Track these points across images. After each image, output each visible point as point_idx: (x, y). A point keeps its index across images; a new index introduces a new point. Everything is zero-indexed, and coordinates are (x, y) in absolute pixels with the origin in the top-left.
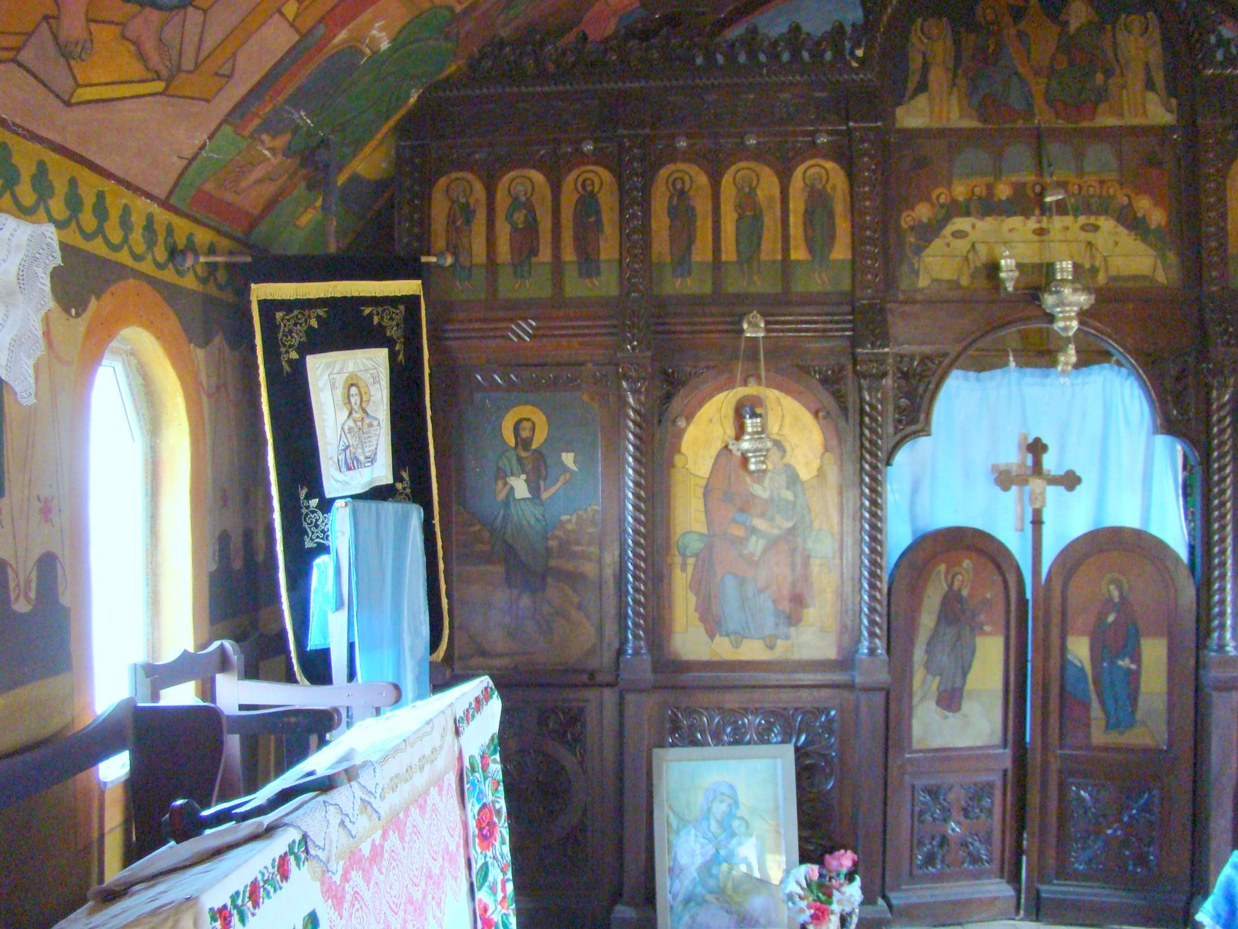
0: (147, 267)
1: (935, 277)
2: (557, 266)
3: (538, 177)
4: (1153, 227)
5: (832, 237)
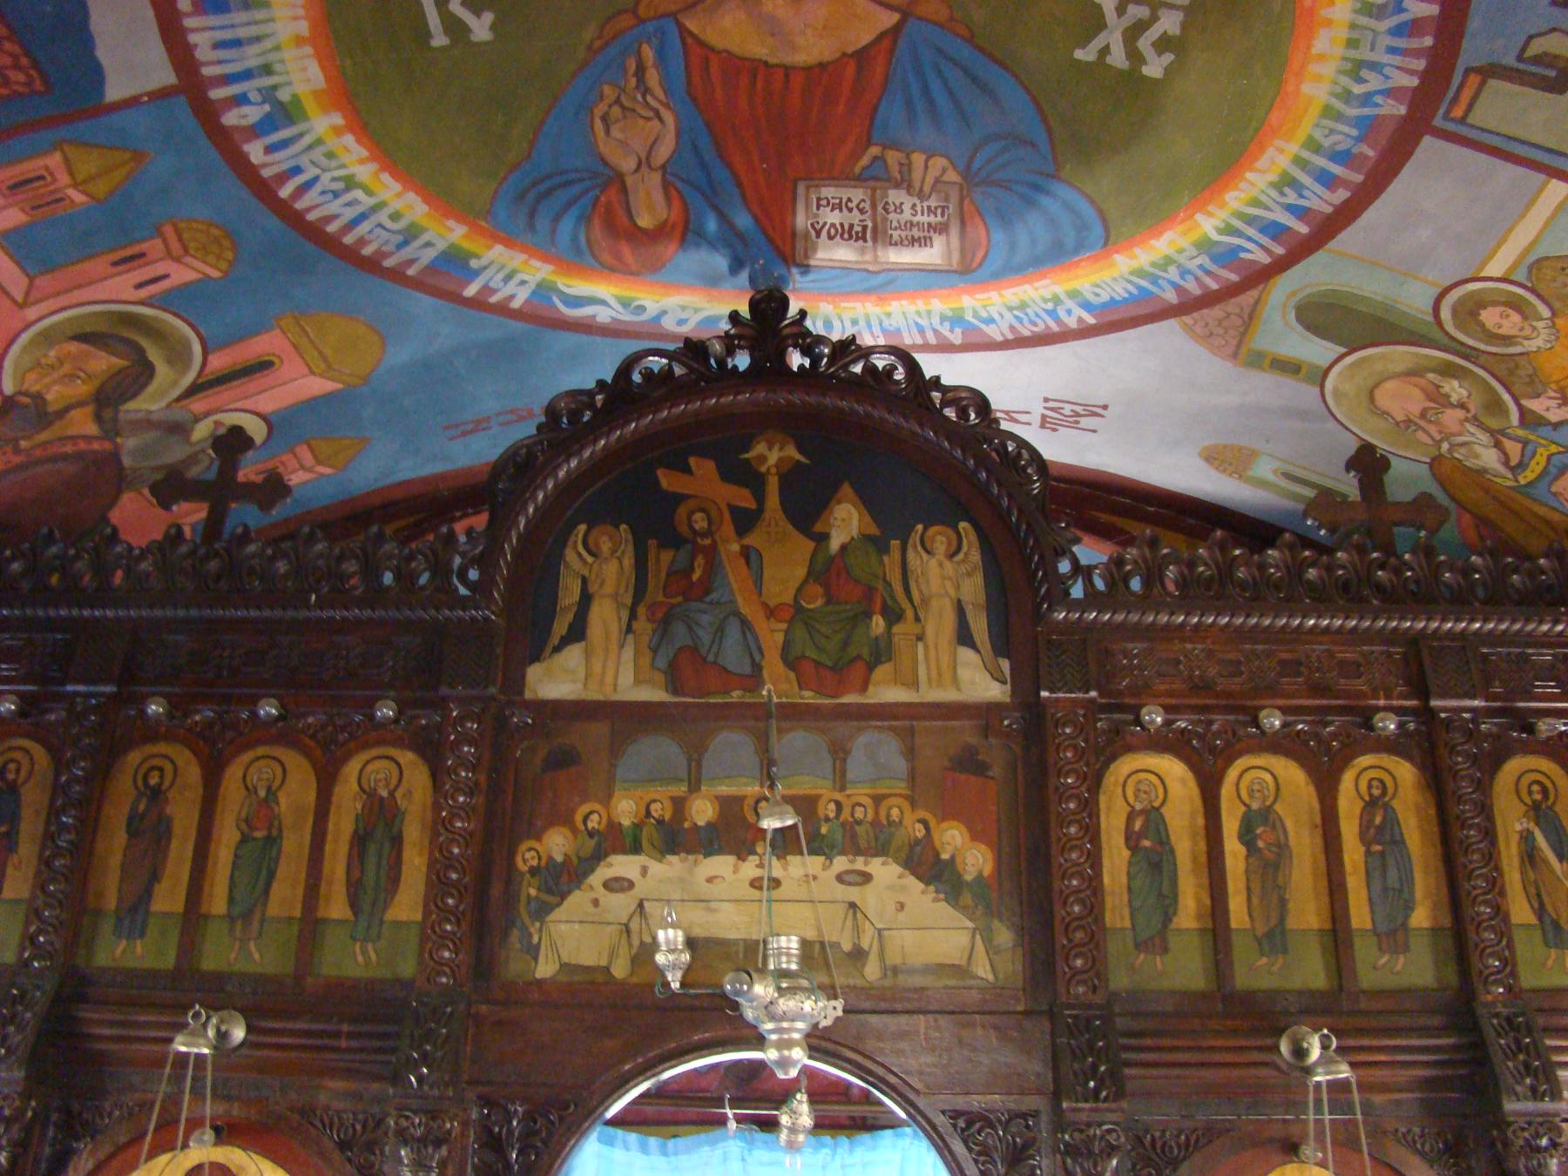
1: (565, 959)
4: (968, 877)
5: (395, 880)
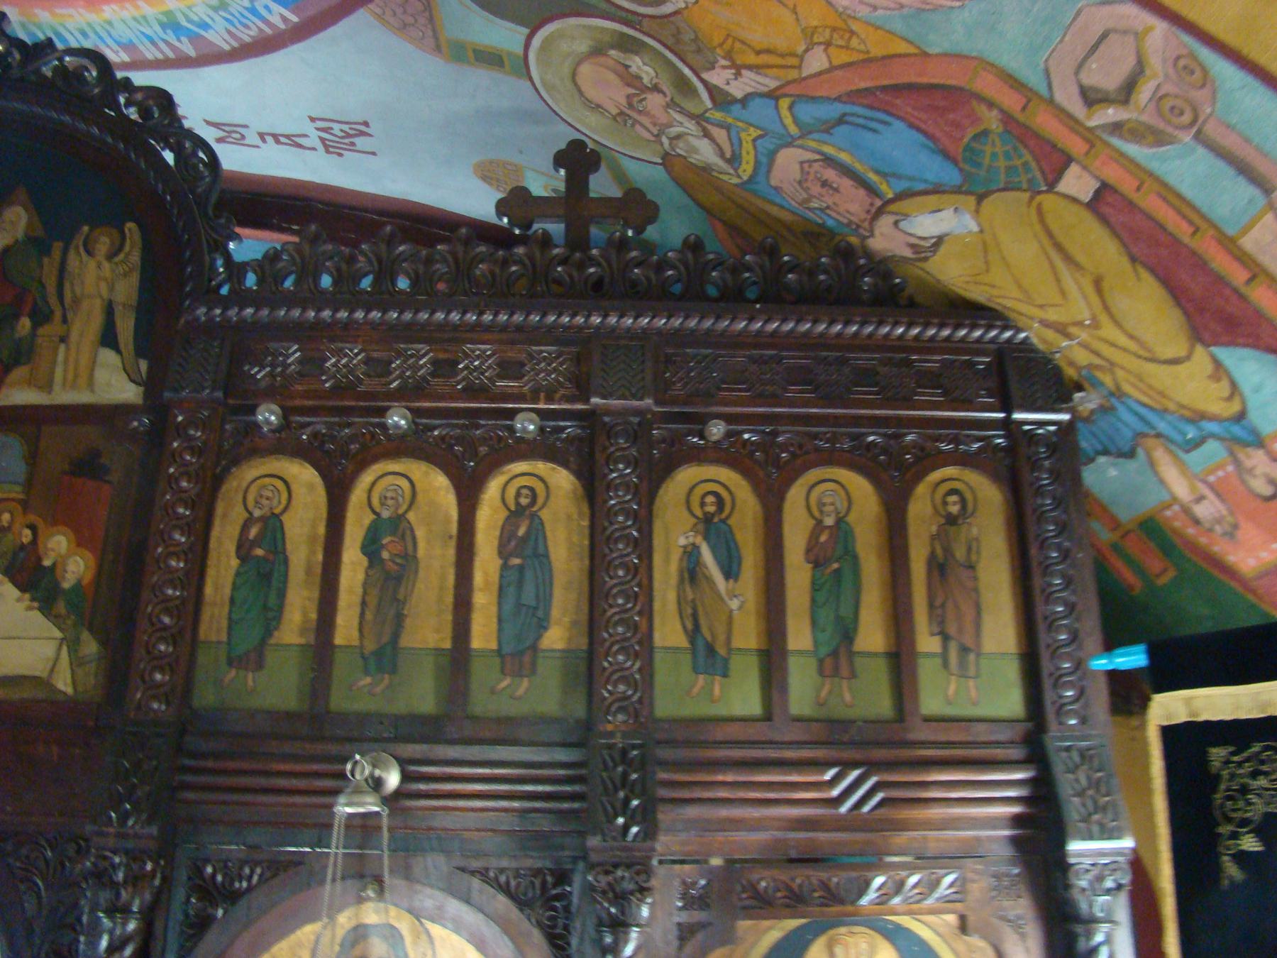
4: (66, 585)
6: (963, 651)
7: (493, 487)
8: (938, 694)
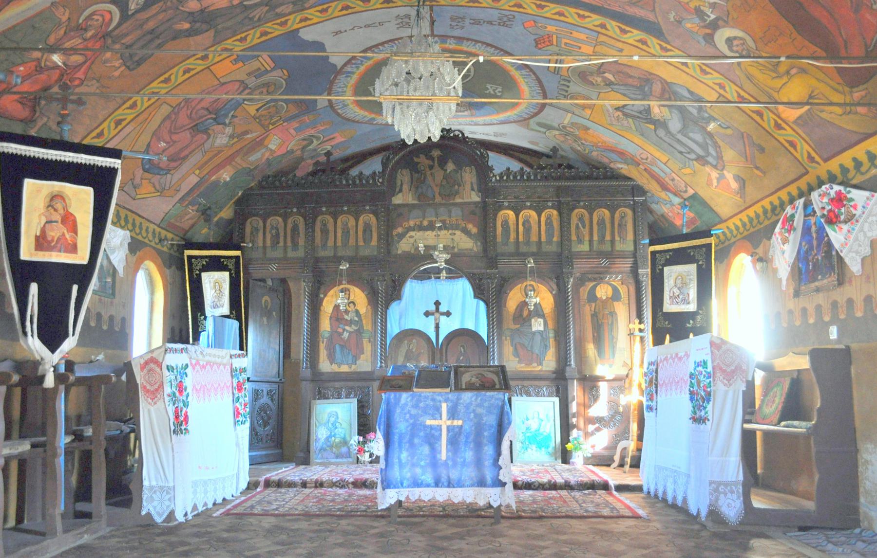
0: (153, 244)
2: (285, 246)
3: (280, 219)
6: (623, 239)
7: (543, 214)
8: (619, 247)
